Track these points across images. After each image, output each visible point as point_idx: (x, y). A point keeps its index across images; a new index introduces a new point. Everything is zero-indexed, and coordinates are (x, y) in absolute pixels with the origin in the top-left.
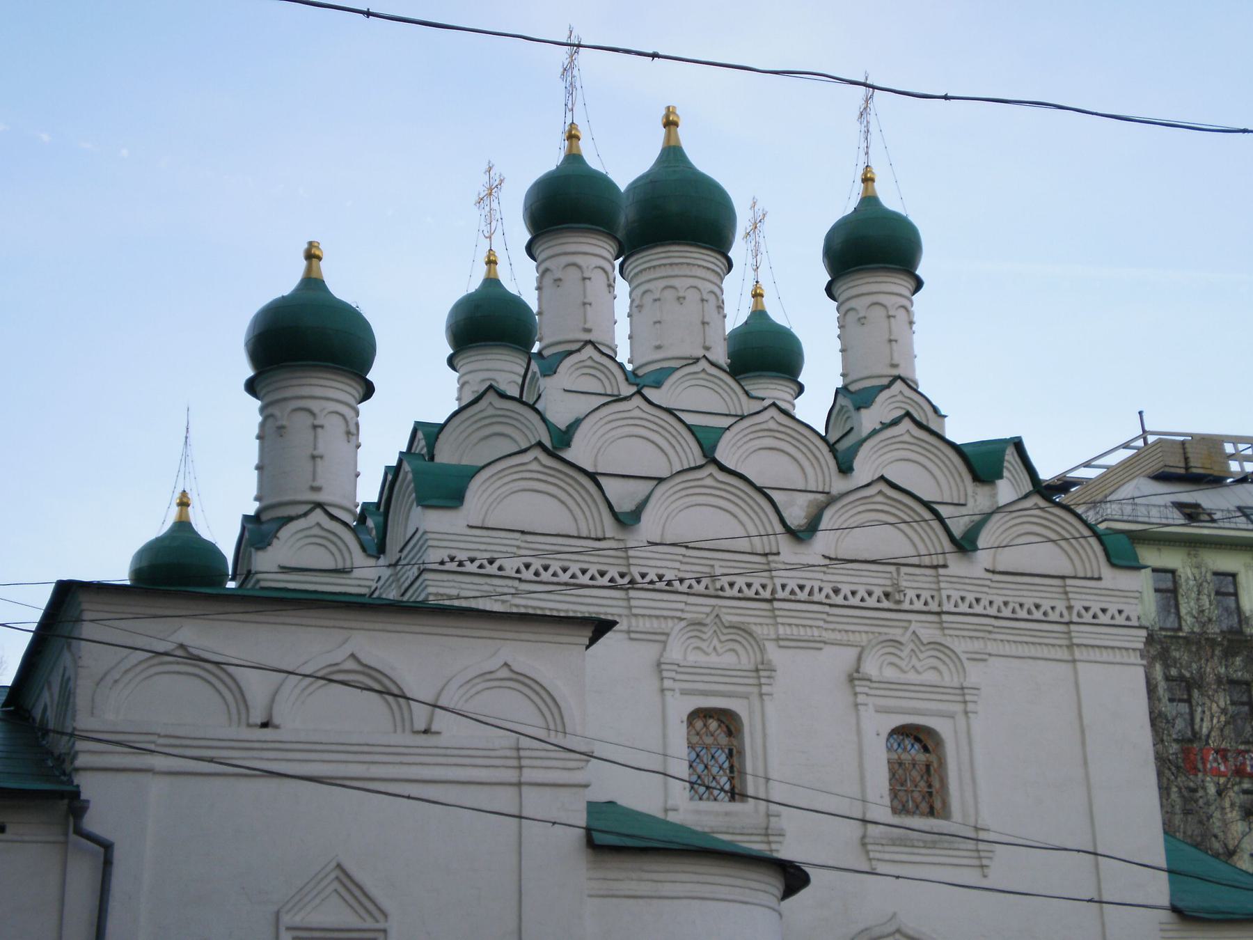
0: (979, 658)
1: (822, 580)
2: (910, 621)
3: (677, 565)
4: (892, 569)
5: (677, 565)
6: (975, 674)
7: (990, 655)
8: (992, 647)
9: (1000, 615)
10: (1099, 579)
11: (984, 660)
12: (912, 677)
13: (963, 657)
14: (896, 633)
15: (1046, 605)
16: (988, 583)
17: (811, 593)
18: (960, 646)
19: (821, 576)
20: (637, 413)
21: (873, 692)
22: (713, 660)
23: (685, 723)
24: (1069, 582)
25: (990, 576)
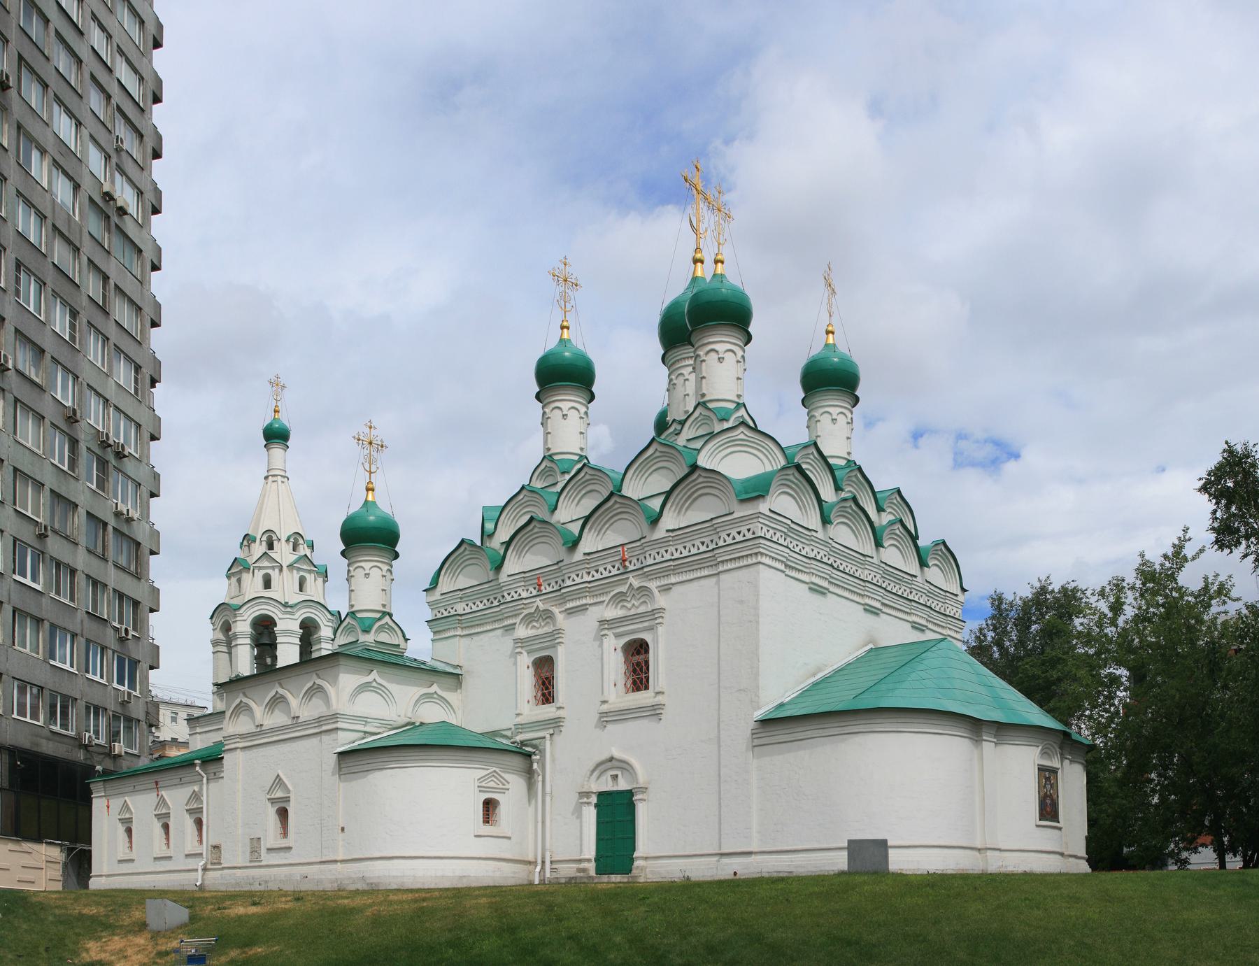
0: (666, 589)
1: (588, 568)
3: (523, 583)
4: (620, 549)
5: (523, 583)
7: (673, 584)
8: (673, 579)
9: (673, 558)
12: (633, 612)
13: (656, 591)
14: (624, 589)
15: (707, 540)
17: (582, 578)
18: (653, 585)
22: (540, 631)
23: (531, 669)
24: (714, 522)
25: (671, 534)
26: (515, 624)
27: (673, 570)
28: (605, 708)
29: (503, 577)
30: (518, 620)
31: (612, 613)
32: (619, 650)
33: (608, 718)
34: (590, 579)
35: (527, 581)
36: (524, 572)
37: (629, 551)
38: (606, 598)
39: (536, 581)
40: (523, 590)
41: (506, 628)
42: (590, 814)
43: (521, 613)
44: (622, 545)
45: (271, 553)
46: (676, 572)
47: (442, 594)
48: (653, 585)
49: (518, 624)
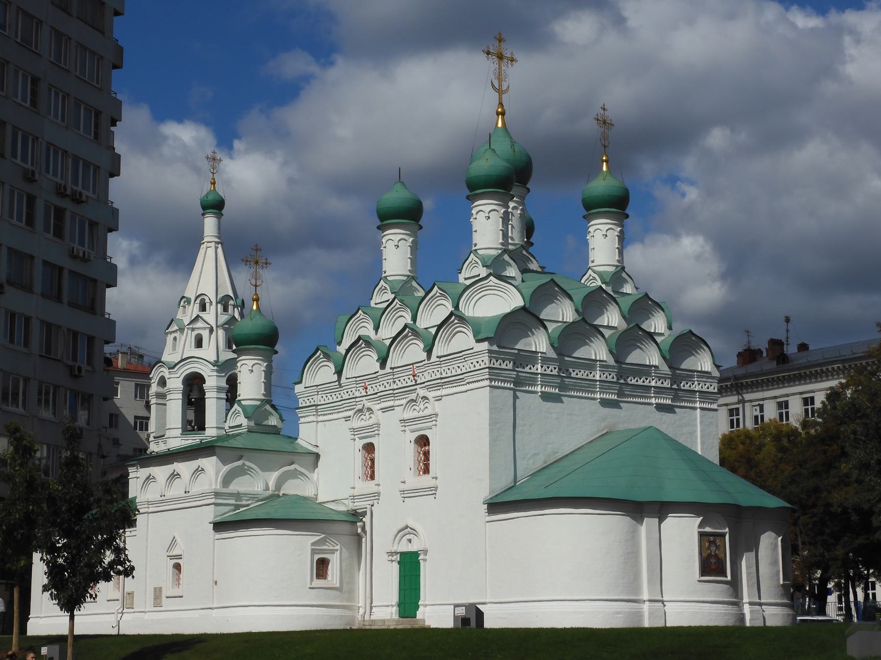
0: (439, 399)
1: (394, 379)
2: (416, 389)
3: (355, 385)
4: (411, 366)
5: (355, 385)
6: (438, 407)
7: (442, 396)
9: (442, 376)
10: (473, 349)
11: (441, 399)
12: (421, 414)
16: (439, 363)
19: (392, 377)
20: (361, 317)
21: (406, 424)
25: (438, 359)
26: (350, 417)
27: (442, 386)
28: (403, 487)
29: (343, 380)
30: (351, 413)
31: (409, 414)
32: (413, 442)
33: (408, 494)
34: (395, 387)
35: (358, 384)
36: (356, 377)
37: (417, 368)
38: (404, 402)
39: (363, 384)
40: (356, 390)
41: (346, 419)
42: (396, 567)
43: (354, 409)
44: (413, 364)
45: (202, 314)
46: (444, 387)
47: (305, 388)
48: (431, 395)
49: (352, 417)
